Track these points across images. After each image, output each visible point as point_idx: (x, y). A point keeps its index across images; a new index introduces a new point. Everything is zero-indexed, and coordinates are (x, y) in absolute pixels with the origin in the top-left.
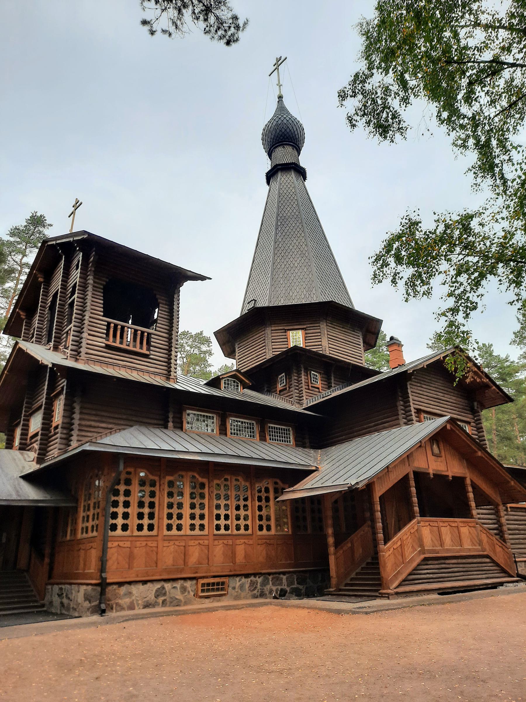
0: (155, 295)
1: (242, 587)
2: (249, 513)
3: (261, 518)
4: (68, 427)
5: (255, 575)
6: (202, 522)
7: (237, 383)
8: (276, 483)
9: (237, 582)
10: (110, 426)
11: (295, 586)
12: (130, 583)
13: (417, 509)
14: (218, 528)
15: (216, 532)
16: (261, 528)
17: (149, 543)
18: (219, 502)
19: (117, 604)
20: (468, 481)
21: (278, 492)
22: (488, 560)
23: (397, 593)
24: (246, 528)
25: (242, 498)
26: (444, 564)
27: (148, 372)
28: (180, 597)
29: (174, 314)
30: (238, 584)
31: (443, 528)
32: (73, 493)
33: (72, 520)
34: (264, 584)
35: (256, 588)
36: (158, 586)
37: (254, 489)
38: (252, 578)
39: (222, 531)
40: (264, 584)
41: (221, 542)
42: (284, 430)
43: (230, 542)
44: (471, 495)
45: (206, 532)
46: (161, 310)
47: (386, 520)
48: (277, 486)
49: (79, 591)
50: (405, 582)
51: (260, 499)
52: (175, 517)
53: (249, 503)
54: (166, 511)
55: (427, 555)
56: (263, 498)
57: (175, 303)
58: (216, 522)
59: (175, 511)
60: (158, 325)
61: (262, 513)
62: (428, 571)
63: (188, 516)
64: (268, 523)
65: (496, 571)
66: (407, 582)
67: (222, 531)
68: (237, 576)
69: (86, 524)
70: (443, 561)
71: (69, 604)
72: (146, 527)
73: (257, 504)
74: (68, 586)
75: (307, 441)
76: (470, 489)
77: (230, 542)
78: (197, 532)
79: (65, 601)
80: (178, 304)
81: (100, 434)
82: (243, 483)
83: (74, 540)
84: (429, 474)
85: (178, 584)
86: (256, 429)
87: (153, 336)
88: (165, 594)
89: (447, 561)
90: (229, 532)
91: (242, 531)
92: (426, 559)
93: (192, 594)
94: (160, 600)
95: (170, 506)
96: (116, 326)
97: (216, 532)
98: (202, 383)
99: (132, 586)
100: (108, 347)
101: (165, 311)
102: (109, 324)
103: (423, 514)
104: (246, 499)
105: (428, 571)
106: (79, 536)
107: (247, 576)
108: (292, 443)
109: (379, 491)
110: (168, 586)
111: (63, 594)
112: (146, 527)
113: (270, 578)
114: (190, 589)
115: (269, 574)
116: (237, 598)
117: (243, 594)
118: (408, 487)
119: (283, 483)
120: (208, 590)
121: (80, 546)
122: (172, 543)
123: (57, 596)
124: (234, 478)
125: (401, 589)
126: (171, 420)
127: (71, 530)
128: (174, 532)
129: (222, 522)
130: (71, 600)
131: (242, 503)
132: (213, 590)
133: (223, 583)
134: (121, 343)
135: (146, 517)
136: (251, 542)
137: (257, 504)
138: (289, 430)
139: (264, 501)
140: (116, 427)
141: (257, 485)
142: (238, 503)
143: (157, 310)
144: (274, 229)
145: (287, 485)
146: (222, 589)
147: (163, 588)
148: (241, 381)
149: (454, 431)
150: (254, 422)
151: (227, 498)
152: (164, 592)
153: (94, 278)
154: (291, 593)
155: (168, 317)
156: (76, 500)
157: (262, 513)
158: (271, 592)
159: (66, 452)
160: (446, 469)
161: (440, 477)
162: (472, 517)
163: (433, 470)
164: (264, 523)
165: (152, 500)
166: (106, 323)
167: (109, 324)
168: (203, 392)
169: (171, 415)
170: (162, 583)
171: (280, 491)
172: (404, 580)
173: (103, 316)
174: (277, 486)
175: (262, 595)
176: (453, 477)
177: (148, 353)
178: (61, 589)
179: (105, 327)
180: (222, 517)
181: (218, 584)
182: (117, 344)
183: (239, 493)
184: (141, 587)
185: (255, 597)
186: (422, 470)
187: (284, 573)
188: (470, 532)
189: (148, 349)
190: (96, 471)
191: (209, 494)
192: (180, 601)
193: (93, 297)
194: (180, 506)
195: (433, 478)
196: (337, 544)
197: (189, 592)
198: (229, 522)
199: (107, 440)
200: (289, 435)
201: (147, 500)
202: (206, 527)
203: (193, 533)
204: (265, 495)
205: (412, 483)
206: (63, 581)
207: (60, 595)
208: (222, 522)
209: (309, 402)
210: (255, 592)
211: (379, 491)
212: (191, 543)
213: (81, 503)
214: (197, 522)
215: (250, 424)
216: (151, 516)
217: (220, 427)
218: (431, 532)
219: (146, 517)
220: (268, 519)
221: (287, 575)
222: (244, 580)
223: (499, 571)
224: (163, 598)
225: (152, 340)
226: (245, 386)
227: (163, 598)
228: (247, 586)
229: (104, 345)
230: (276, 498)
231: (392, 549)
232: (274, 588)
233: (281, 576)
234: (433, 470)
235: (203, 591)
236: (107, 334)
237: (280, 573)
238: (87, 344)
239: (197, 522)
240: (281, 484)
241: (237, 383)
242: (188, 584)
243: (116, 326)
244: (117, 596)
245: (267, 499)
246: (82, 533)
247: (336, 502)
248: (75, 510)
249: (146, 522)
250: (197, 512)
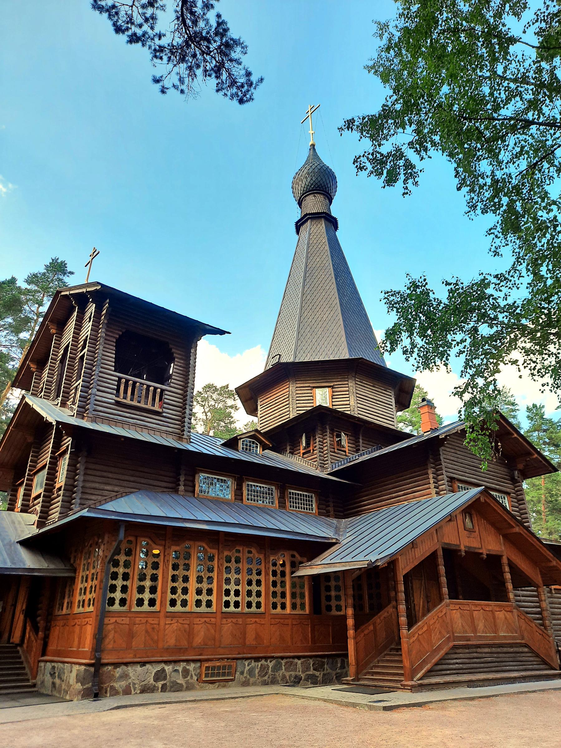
0: (171, 349)
1: (251, 672)
2: (262, 589)
3: (274, 594)
4: (70, 488)
5: (266, 658)
6: (209, 598)
7: (256, 444)
8: (293, 556)
9: (247, 666)
10: (116, 489)
11: (311, 672)
12: (126, 664)
13: (445, 590)
15: (224, 610)
17: (150, 620)
18: (229, 576)
19: (112, 688)
20: (505, 560)
21: (295, 566)
22: (526, 650)
23: (421, 685)
24: (258, 605)
25: (254, 572)
26: (476, 652)
27: (160, 431)
28: (181, 681)
29: (190, 370)
30: (247, 668)
31: (476, 612)
32: (72, 562)
33: (70, 591)
34: (277, 668)
35: (266, 673)
36: (159, 667)
37: (269, 562)
38: (263, 662)
39: (232, 609)
40: (277, 668)
41: (230, 620)
42: (306, 497)
43: (240, 621)
44: (508, 576)
46: (176, 365)
47: (414, 601)
48: (293, 559)
49: (71, 672)
50: (430, 673)
51: (274, 573)
52: (179, 591)
53: (262, 578)
54: (170, 585)
55: (456, 643)
56: (279, 572)
57: (191, 358)
59: (180, 585)
60: (172, 380)
61: (276, 589)
62: (458, 661)
63: (194, 592)
64: (283, 600)
65: (535, 663)
66: (434, 673)
67: (232, 609)
68: (247, 659)
69: (83, 597)
70: (474, 650)
71: (61, 686)
72: (146, 602)
73: (272, 578)
74: (61, 665)
75: (331, 509)
76: (507, 569)
78: (203, 609)
79: (57, 681)
80: (195, 359)
81: (105, 498)
82: (255, 554)
83: (69, 614)
84: (460, 550)
85: (180, 667)
86: (276, 494)
87: (166, 392)
88: (165, 678)
89: (479, 650)
90: (240, 609)
91: (254, 609)
92: (455, 647)
93: (195, 678)
94: (160, 684)
95: (174, 579)
96: (127, 381)
97: (224, 610)
98: (219, 443)
99: (129, 668)
100: (118, 403)
101: (180, 366)
102: (120, 379)
103: (453, 595)
104: (259, 574)
105: (458, 661)
106: (76, 610)
108: (314, 511)
109: (403, 569)
110: (168, 668)
111: (55, 673)
112: (146, 602)
113: (283, 662)
114: (193, 673)
115: (282, 658)
116: (245, 684)
118: (437, 565)
119: (301, 556)
120: (213, 675)
121: (76, 620)
122: (175, 620)
123: (49, 675)
124: (247, 550)
125: (426, 681)
126: (182, 483)
127: (68, 603)
128: (178, 608)
129: (232, 598)
130: (63, 681)
131: (255, 578)
132: (218, 675)
133: (230, 667)
134: (132, 400)
135: (147, 590)
137: (272, 578)
138: (311, 496)
139: (279, 575)
140: (122, 490)
141: (272, 558)
142: (250, 577)
143: (172, 365)
144: (302, 281)
145: (306, 559)
146: (229, 674)
147: (163, 670)
148: (261, 442)
149: (489, 504)
150: (274, 487)
151: (238, 571)
152: (163, 675)
153: (106, 330)
154: (307, 679)
155: (184, 373)
156: (75, 571)
157: (276, 589)
158: (284, 677)
159: (67, 516)
160: (480, 546)
161: (473, 555)
162: (507, 600)
163: (465, 547)
164: (278, 600)
165: (155, 572)
166: (117, 379)
167: (120, 379)
168: (218, 454)
169: (182, 478)
170: (163, 665)
171: (297, 563)
172: (430, 671)
173: (115, 371)
174: (293, 559)
175: (274, 682)
176: (487, 555)
177: (160, 410)
178: (54, 668)
179: (116, 383)
180: (232, 593)
181: (224, 667)
182: (128, 401)
183: (250, 566)
184: (139, 668)
185: (265, 683)
186: (452, 548)
187: (299, 658)
188: (506, 618)
189: (161, 407)
190: (96, 539)
191: (218, 567)
192: (181, 685)
193: (103, 351)
194: (186, 579)
195: (465, 556)
196: (357, 627)
197: (192, 676)
198: (239, 599)
199: (110, 506)
200: (312, 502)
201: (149, 572)
204: (281, 569)
205: (441, 561)
206: (56, 659)
207: (52, 675)
208: (232, 598)
209: (334, 466)
210: (266, 678)
211: (403, 569)
212: (197, 621)
213: (79, 573)
214: (204, 598)
215: (269, 489)
216: (153, 590)
217: (235, 492)
218: (462, 616)
219: (147, 590)
220: (283, 595)
221: (302, 660)
222: (253, 664)
223: (538, 663)
224: (162, 682)
225: (166, 396)
226: (265, 447)
227: (162, 682)
228: (257, 671)
229: (113, 401)
230: (293, 573)
231: (417, 635)
232: (287, 674)
233: (296, 660)
234: (465, 547)
235: (207, 675)
236: (118, 390)
237: (294, 657)
238: (96, 400)
239: (204, 598)
240: (298, 558)
241: (256, 444)
242: (191, 667)
243: (127, 381)
244: (112, 678)
245: (283, 574)
246: (79, 607)
247: (359, 578)
248: (72, 580)
249: (147, 596)
250: (205, 586)
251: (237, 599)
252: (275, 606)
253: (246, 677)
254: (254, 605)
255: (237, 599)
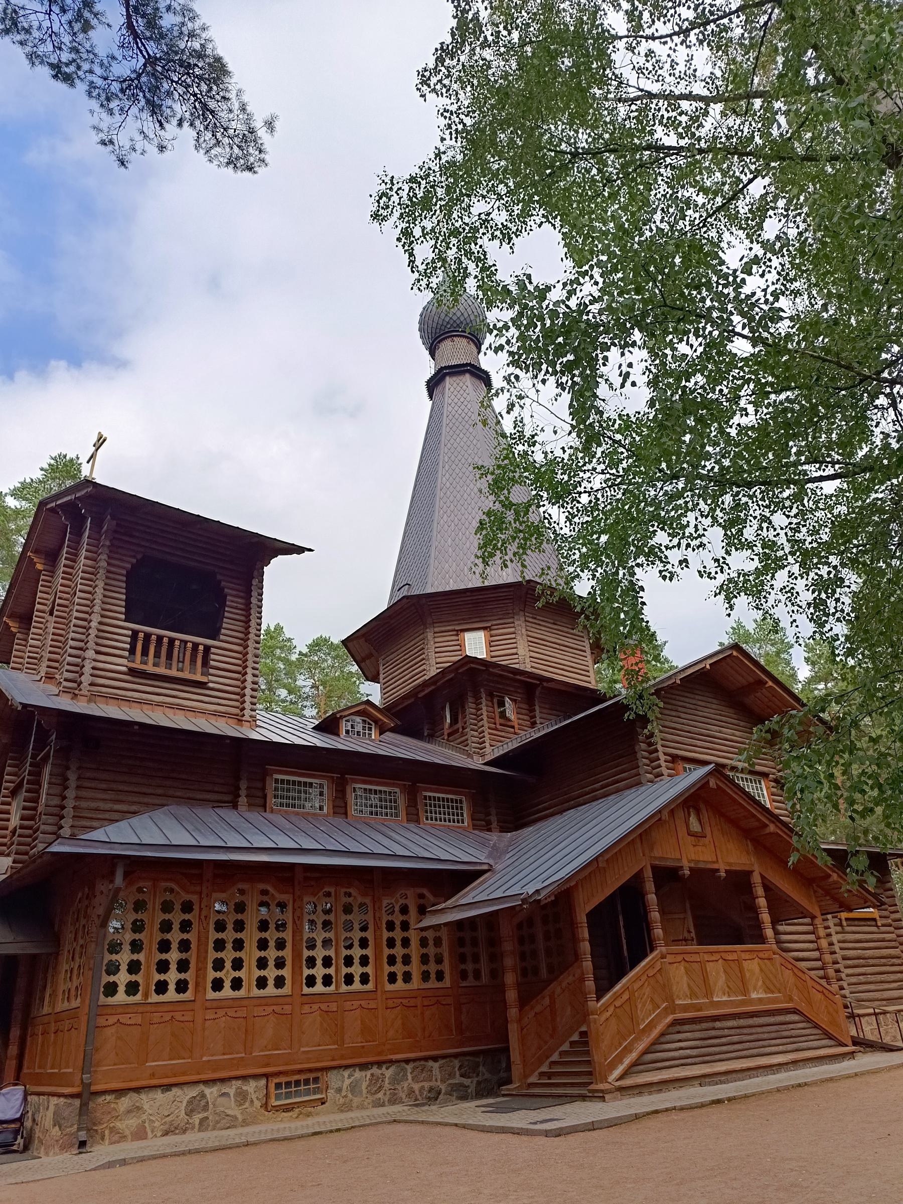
5: (379, 1064)
14: (311, 981)
15: (306, 990)
16: (392, 978)
24: (365, 979)
30: (347, 1082)
39: (319, 988)
41: (315, 1007)
43: (333, 1007)
45: (286, 990)
58: (307, 972)
63: (254, 963)
67: (319, 988)
77: (333, 1007)
82: (357, 897)
90: (333, 987)
97: (306, 990)
107: (364, 1066)
113: (409, 1068)
115: (407, 1061)
117: (356, 1101)
129: (319, 971)
136: (373, 1005)
187: (435, 1059)
198: (331, 971)
202: (288, 982)
203: (262, 993)
208: (319, 971)
210: (380, 1095)
228: (364, 1085)
251: (328, 971)
252: (392, 978)
253: (346, 1096)
254: (357, 979)
255: (328, 971)
